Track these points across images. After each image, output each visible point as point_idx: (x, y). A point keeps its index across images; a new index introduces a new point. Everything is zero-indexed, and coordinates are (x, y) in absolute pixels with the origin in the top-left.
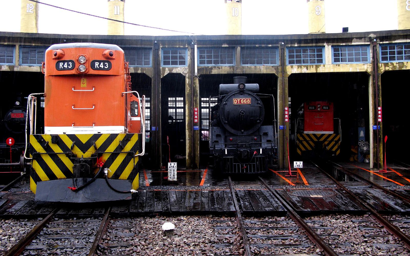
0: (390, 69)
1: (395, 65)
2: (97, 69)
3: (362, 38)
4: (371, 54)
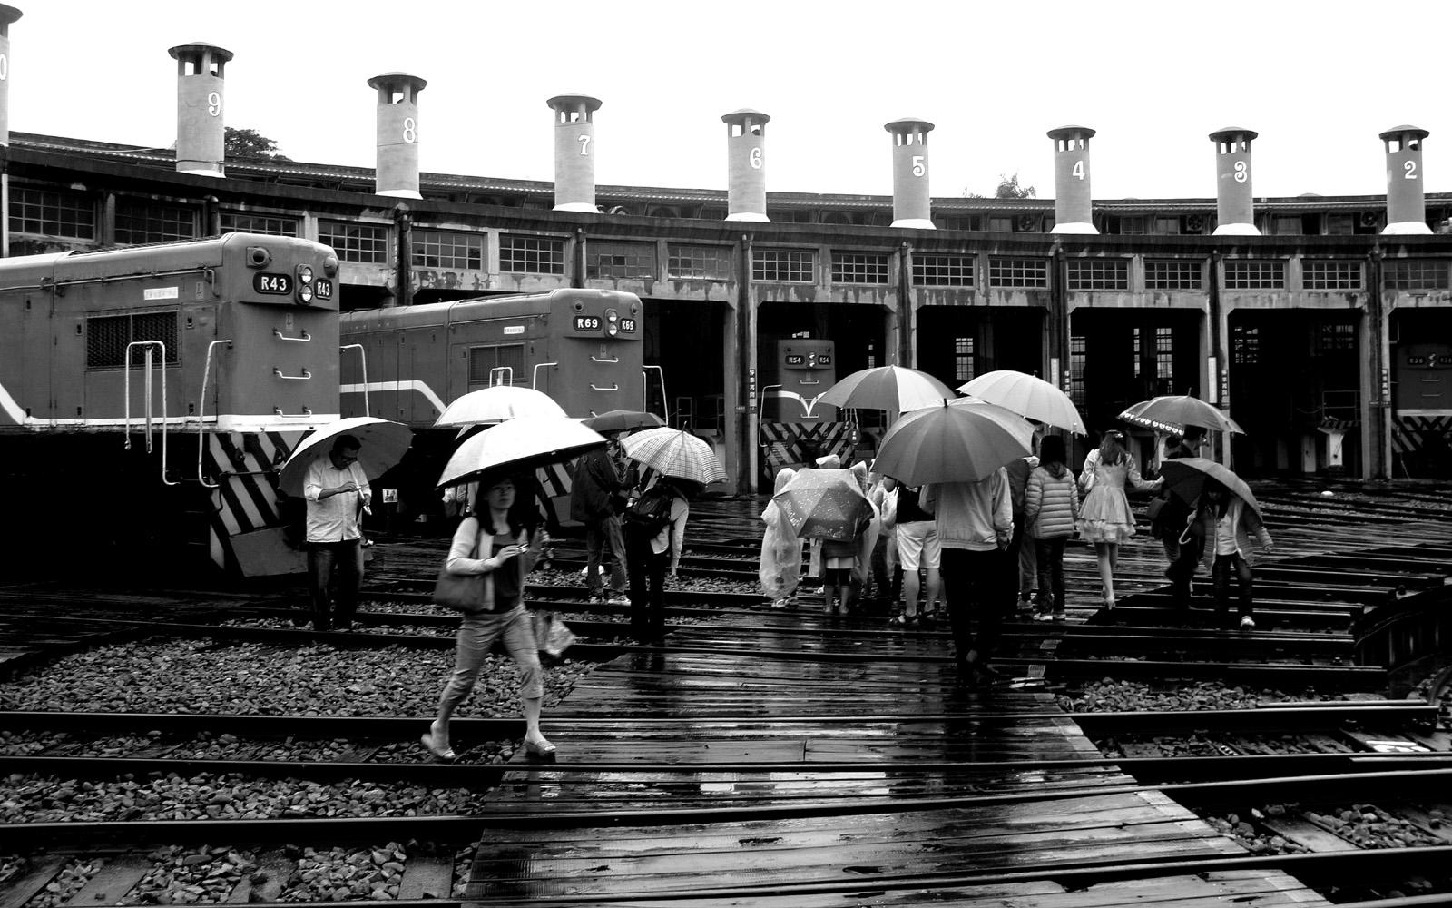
0: (431, 286)
1: (440, 277)
2: (265, 292)
4: (396, 248)
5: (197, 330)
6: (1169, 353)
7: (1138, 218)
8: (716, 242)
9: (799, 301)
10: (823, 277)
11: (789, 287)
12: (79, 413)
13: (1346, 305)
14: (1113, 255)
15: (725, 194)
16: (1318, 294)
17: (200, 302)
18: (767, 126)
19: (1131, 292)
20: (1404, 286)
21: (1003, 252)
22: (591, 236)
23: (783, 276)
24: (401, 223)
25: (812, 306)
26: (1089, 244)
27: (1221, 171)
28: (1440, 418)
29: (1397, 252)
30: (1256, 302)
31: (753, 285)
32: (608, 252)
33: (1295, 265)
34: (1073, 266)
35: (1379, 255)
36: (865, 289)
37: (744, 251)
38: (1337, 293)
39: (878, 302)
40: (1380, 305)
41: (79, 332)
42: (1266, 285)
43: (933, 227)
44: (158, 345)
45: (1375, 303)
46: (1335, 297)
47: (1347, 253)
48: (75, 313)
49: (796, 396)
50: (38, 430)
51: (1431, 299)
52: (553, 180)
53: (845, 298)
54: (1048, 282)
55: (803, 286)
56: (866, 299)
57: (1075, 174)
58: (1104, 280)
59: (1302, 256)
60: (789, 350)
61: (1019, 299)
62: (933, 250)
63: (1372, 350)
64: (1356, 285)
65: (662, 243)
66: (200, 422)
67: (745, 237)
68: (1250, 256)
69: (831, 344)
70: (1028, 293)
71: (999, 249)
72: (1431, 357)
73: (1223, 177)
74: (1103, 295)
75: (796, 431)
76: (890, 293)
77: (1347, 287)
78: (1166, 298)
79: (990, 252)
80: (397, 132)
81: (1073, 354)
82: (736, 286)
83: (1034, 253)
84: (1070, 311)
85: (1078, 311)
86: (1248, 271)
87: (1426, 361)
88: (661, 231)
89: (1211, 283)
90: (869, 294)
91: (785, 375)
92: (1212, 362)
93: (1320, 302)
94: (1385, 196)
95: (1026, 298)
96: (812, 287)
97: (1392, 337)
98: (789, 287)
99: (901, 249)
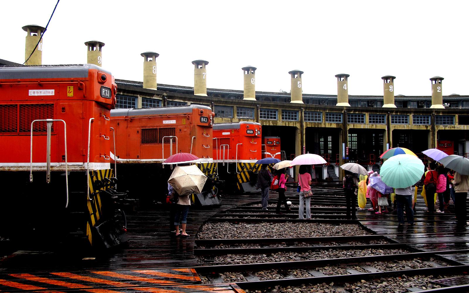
3: (159, 95)
5: (183, 133)
6: (356, 141)
7: (357, 101)
8: (250, 107)
9: (273, 125)
10: (280, 118)
11: (270, 121)
12: (138, 158)
13: (425, 129)
14: (360, 113)
15: (243, 92)
16: (417, 125)
17: (183, 125)
18: (256, 71)
19: (365, 124)
20: (441, 124)
22: (216, 104)
23: (268, 118)
24: (164, 99)
25: (276, 126)
26: (354, 110)
27: (385, 88)
29: (439, 114)
30: (400, 127)
31: (260, 120)
32: (220, 109)
33: (411, 117)
34: (349, 116)
35: (435, 114)
36: (291, 122)
37: (258, 110)
38: (422, 125)
39: (295, 126)
40: (435, 129)
41: (138, 133)
42: (403, 122)
43: (349, 106)
44: (175, 138)
45: (433, 128)
46: (422, 126)
47: (425, 114)
48: (137, 127)
49: (269, 154)
50: (122, 162)
51: (449, 127)
52: (243, 90)
53: (286, 124)
54: (342, 121)
55: (274, 121)
56: (291, 125)
57: (344, 88)
58: (351, 120)
59: (413, 114)
60: (268, 140)
61: (334, 126)
62: (310, 111)
63: (432, 142)
64: (428, 123)
65: (235, 107)
66: (236, 161)
67: (258, 106)
68: (398, 114)
69: (279, 138)
71: (328, 111)
72: (446, 144)
73: (386, 90)
76: (298, 123)
77: (425, 123)
78: (375, 126)
79: (326, 111)
80: (151, 70)
81: (349, 141)
82: (255, 120)
83: (338, 112)
84: (348, 129)
85: (350, 129)
86: (401, 118)
88: (235, 103)
89: (388, 122)
90: (292, 123)
92: (388, 145)
93: (418, 128)
94: (431, 96)
95: (336, 125)
96: (276, 121)
97: (438, 138)
99: (301, 110)
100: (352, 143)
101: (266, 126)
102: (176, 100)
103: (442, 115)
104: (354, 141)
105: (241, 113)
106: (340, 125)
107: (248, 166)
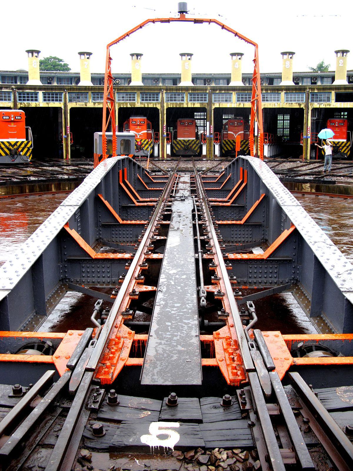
11: (127, 103)
13: (298, 107)
16: (290, 103)
20: (316, 101)
21: (192, 92)
22: (69, 91)
25: (134, 108)
28: (339, 142)
32: (74, 95)
36: (150, 103)
39: (155, 106)
42: (274, 101)
56: (151, 106)
69: (145, 118)
70: (200, 103)
74: (223, 104)
75: (232, 142)
85: (216, 109)
87: (234, 124)
91: (132, 127)
96: (135, 103)
98: (127, 103)
100: (283, 122)
101: (123, 108)
102: (26, 91)
103: (317, 91)
104: (286, 120)
105: (98, 98)
106: (204, 105)
107: (7, 145)
